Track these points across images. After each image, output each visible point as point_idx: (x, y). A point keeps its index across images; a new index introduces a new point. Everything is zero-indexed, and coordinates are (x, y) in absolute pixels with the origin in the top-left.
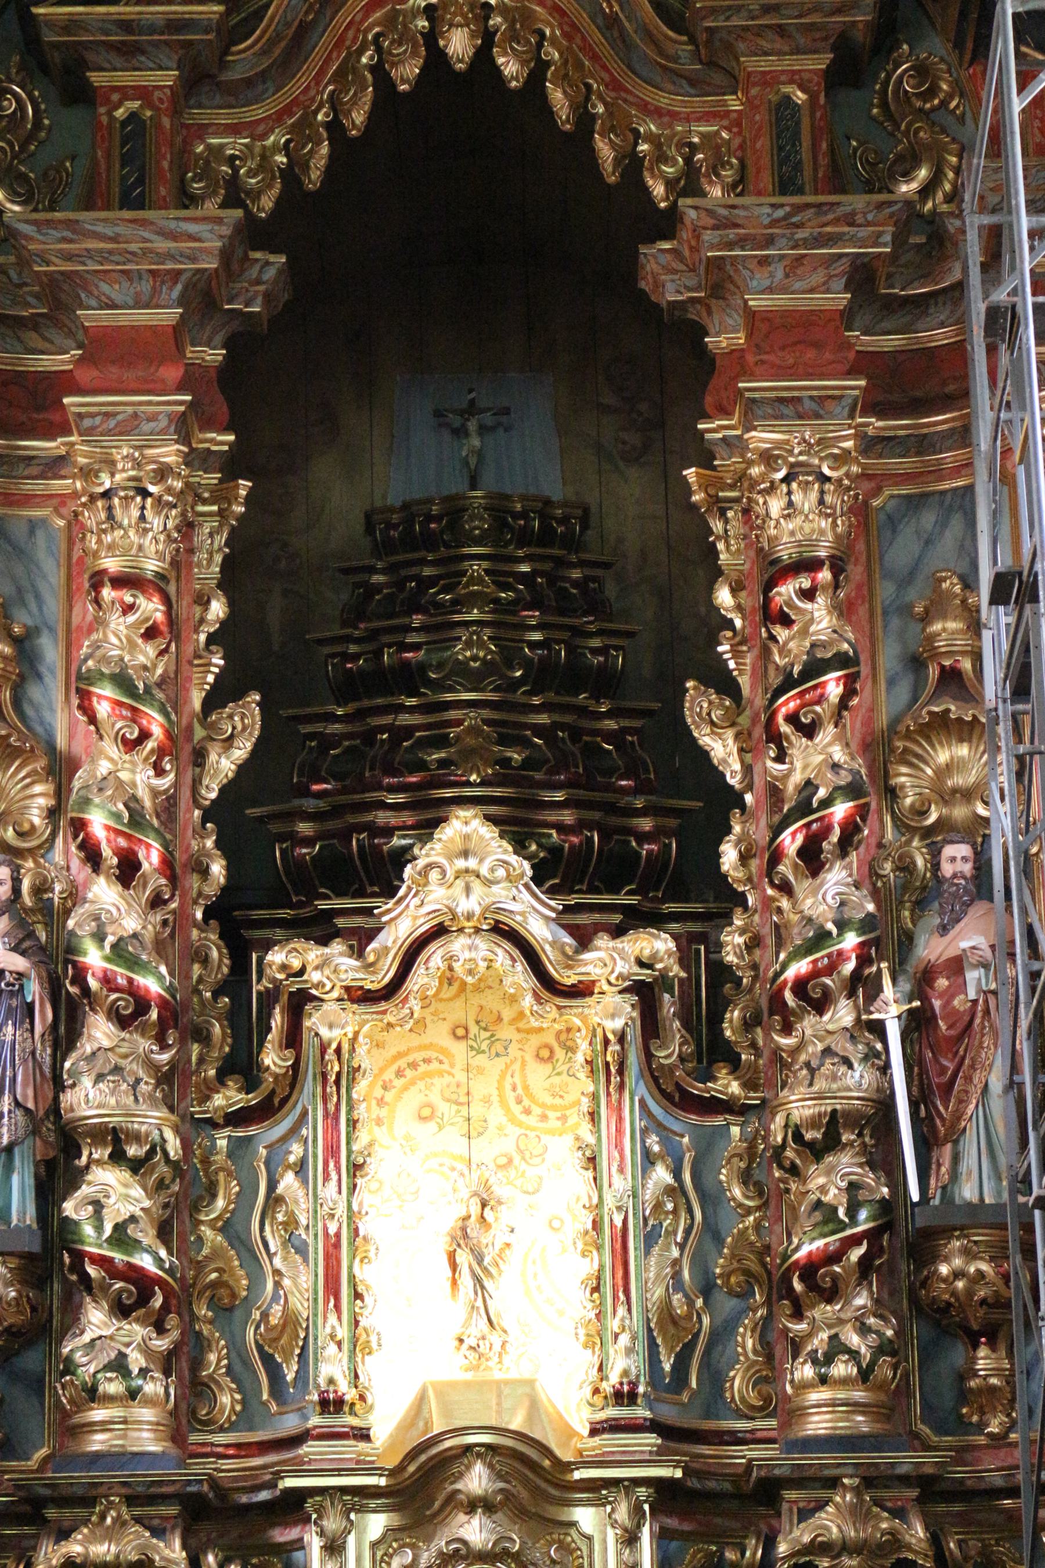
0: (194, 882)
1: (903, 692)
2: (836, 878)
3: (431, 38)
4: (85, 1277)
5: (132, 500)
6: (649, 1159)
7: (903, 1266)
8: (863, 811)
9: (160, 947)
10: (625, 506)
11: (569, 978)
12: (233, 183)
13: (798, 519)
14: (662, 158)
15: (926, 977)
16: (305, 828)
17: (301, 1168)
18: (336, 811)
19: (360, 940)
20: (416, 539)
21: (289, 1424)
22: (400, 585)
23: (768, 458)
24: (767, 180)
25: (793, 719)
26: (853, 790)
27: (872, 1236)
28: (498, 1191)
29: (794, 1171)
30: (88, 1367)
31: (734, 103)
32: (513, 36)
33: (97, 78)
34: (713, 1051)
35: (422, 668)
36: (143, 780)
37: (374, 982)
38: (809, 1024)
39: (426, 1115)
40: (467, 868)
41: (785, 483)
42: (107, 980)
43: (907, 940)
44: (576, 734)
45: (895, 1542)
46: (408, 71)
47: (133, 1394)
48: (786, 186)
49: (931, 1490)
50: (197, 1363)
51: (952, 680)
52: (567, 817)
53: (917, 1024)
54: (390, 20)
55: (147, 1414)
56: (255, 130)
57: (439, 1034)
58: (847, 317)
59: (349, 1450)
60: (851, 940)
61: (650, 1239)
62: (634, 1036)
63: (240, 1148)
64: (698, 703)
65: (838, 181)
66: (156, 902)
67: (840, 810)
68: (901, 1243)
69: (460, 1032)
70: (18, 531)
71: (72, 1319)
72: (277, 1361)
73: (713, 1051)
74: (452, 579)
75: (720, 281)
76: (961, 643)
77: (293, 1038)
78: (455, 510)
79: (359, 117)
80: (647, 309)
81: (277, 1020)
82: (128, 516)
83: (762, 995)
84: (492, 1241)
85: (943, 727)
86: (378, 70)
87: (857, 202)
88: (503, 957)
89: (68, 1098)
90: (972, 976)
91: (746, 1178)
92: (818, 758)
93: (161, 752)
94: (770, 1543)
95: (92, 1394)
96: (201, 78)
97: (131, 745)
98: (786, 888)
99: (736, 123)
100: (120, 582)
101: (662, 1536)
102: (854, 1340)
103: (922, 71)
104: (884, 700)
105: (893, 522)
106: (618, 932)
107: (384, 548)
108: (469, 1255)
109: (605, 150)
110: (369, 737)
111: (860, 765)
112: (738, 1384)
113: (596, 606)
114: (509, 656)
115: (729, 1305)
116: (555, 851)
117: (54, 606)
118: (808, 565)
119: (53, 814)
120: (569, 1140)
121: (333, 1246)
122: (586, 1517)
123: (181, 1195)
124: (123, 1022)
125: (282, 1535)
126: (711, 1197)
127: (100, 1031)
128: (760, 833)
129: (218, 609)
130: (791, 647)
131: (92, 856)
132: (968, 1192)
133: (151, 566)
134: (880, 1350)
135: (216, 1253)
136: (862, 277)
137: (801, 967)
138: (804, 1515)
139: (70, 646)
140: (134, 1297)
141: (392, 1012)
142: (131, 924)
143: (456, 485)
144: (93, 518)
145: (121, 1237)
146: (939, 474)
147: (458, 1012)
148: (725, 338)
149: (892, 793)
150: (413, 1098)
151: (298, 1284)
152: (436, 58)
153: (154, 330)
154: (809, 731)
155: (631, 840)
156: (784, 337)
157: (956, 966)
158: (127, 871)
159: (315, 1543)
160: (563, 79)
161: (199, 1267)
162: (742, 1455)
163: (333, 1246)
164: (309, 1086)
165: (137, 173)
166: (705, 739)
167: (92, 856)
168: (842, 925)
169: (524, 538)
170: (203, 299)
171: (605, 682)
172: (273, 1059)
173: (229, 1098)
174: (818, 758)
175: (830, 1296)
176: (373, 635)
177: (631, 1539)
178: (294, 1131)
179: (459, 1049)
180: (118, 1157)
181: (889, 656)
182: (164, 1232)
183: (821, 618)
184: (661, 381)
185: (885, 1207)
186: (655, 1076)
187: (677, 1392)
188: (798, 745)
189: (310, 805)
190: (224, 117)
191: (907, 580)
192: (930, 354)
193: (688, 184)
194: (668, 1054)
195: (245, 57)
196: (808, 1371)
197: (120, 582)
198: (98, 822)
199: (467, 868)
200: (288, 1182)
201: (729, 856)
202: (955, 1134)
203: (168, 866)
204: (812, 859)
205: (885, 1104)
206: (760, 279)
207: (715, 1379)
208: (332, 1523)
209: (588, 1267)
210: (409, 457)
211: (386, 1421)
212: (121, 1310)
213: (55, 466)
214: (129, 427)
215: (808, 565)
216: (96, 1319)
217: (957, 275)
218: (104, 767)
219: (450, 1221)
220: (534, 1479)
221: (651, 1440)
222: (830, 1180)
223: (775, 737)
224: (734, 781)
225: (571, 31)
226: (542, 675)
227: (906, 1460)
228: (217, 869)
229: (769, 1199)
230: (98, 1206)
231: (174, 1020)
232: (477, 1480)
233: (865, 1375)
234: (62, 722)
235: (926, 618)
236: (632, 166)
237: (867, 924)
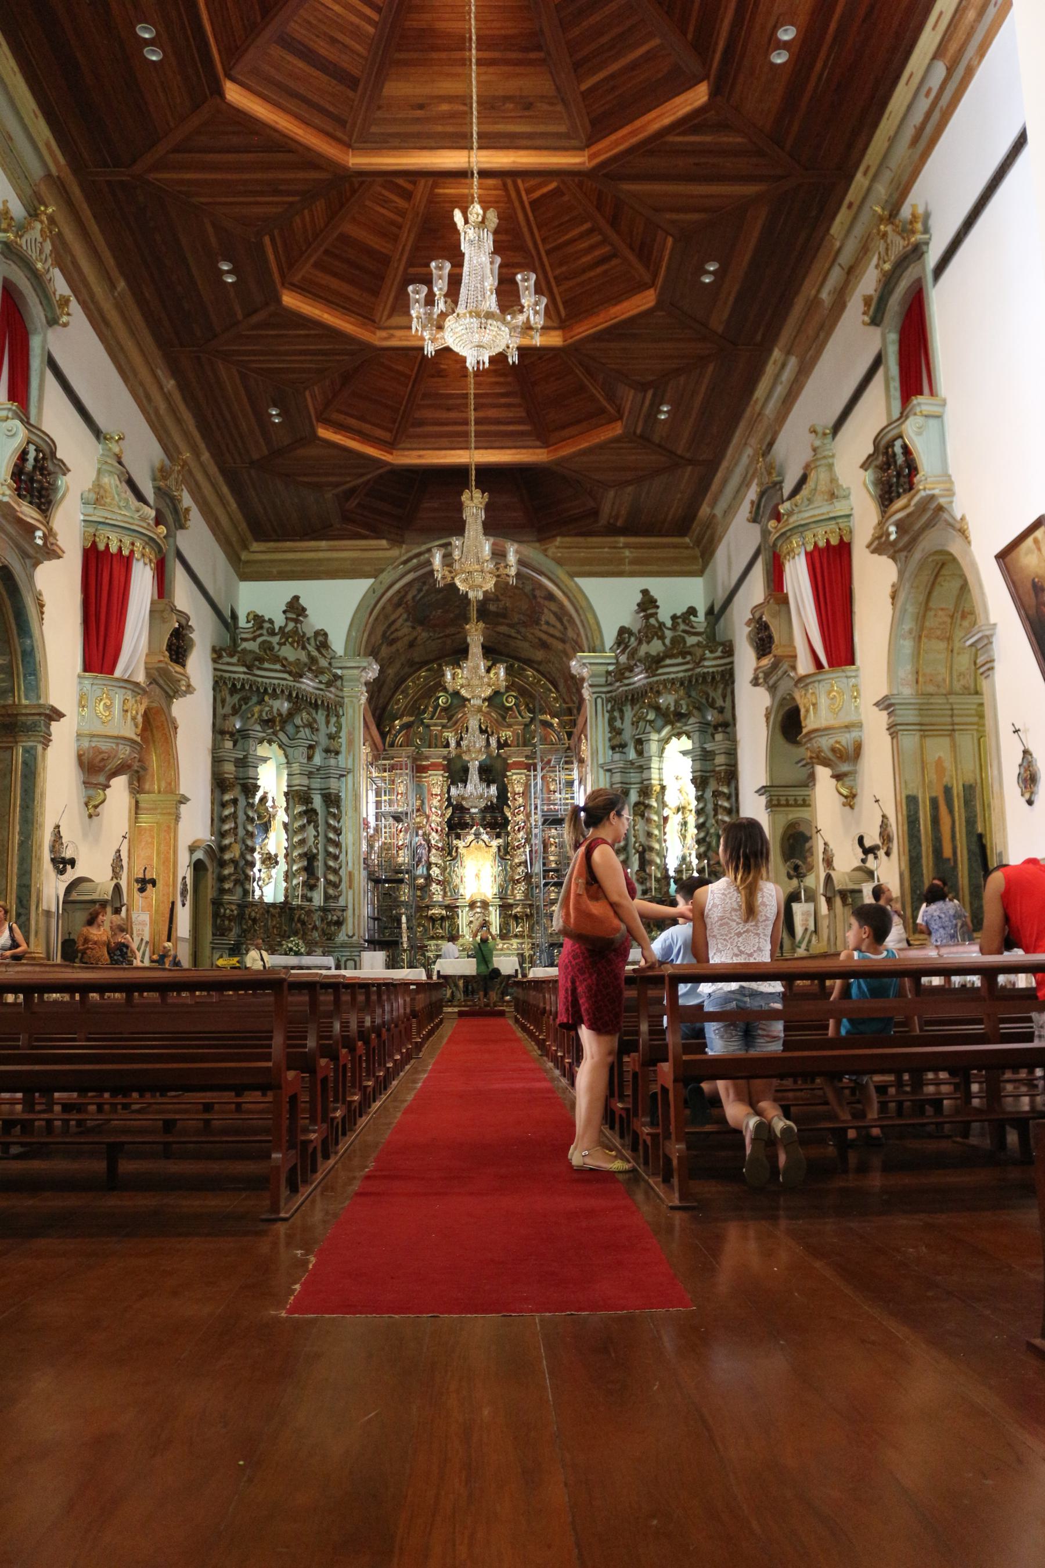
2: (522, 833)
13: (519, 789)
34: (507, 853)
49: (531, 906)
53: (531, 851)
68: (528, 877)
72: (455, 890)
73: (507, 853)
123: (443, 870)
127: (434, 851)
139: (429, 800)
140: (439, 883)
151: (457, 881)
158: (437, 831)
172: (454, 854)
173: (449, 858)
187: (502, 895)
198: (433, 825)
211: (468, 898)
216: (434, 885)
220: (485, 905)
222: (521, 869)
232: (479, 904)
234: (427, 811)
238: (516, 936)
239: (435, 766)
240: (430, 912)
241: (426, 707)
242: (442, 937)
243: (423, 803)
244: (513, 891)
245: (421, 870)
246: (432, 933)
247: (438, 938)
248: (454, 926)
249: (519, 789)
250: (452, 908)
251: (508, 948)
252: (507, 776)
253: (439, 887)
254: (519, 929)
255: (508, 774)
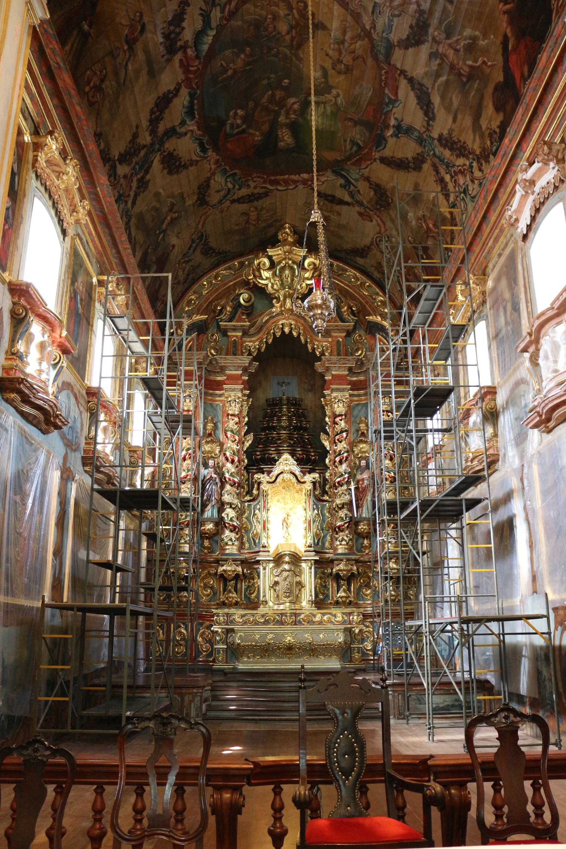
0: (242, 463)
1: (355, 435)
3: (282, 329)
4: (226, 527)
5: (234, 401)
6: (314, 509)
7: (354, 527)
8: (349, 455)
9: (237, 473)
10: (309, 399)
11: (302, 481)
12: (250, 350)
13: (340, 408)
14: (318, 348)
15: (358, 482)
16: (258, 453)
17: (259, 509)
18: (263, 451)
19: (269, 473)
20: (274, 404)
21: (257, 549)
22: (272, 412)
23: (335, 398)
24: (335, 353)
25: (338, 440)
26: (347, 452)
27: (349, 522)
28: (290, 514)
29: (337, 512)
30: (226, 540)
31: (330, 340)
32: (295, 329)
33: (229, 334)
34: (324, 492)
35: (276, 426)
36: (235, 447)
37: (271, 481)
38: (339, 489)
39: (278, 501)
40: (286, 463)
41: (337, 401)
42: (229, 479)
43: (355, 475)
44: (301, 438)
45: (351, 569)
46: (278, 334)
47: (233, 544)
48: (339, 355)
49: (357, 561)
50: (242, 540)
51: (363, 434)
52: (300, 453)
53: (357, 489)
54: (275, 326)
55: (235, 547)
56: (254, 342)
57: (281, 488)
58: (348, 375)
59: (266, 554)
60: (347, 475)
61: (314, 522)
62: (312, 490)
63: (249, 506)
64: (323, 436)
65: (346, 355)
66: (237, 467)
67: (345, 455)
68: (353, 523)
69: (284, 488)
70: (215, 406)
71: (223, 533)
72: (255, 540)
73: (324, 492)
74: (281, 411)
75: (328, 369)
76: (365, 428)
77: (258, 489)
78: (281, 399)
79: (271, 341)
80: (314, 371)
81: (256, 486)
82: (233, 405)
83: (332, 483)
84: (289, 522)
85: (361, 442)
86: (274, 333)
87: (350, 358)
88: (291, 477)
89: (223, 498)
90: (366, 482)
91: (329, 512)
92: (342, 446)
93: (238, 443)
94: (332, 569)
95: (227, 544)
96: (246, 333)
97: (233, 442)
98: (336, 467)
99: (330, 343)
100: (232, 415)
101: (315, 568)
102: (346, 538)
103: (360, 336)
104: (352, 437)
105: (354, 408)
106: (310, 473)
107: (269, 405)
108: (285, 522)
109: (309, 346)
110: (268, 438)
111: (348, 447)
112: (327, 544)
113: (304, 416)
114: (290, 425)
115: (325, 532)
116: (298, 458)
117: (220, 418)
118: (341, 415)
119: (220, 452)
120: (301, 506)
121: (264, 522)
122: (304, 565)
123: (240, 513)
124: (232, 486)
125: (256, 566)
126: (323, 515)
127: (228, 487)
128: (332, 457)
129: (246, 419)
130: (338, 428)
131: (227, 459)
132: (364, 515)
133: (237, 413)
134: (350, 540)
135: (245, 522)
136: (350, 369)
137: (339, 479)
138: (337, 565)
139: (223, 424)
140: (233, 529)
141: (274, 485)
142: (233, 470)
143: (281, 395)
144: (227, 405)
145: (231, 520)
146: (361, 400)
147: (284, 485)
148: (328, 378)
149: (353, 452)
150: (276, 498)
151: (259, 528)
152: (283, 332)
153: (237, 375)
154: (341, 442)
155: (312, 458)
156: (338, 379)
157: (363, 480)
158: (233, 462)
159: (261, 568)
160: (303, 335)
161: (243, 524)
162: (327, 556)
163: (264, 522)
164: (261, 497)
165: (235, 349)
166: (324, 442)
167: (227, 459)
168: (345, 473)
169: (292, 404)
170: (245, 370)
171: (305, 429)
172: (255, 492)
173: (248, 498)
174: (342, 446)
175: (342, 531)
176: (268, 421)
177: (311, 568)
178: (258, 503)
179: (284, 491)
180: (231, 507)
181: (353, 430)
182: (237, 519)
183: (343, 424)
184: (318, 384)
185: (351, 518)
186: (315, 496)
187: (318, 546)
188: (339, 444)
189: (259, 449)
190: (249, 339)
191: (356, 417)
192: (360, 381)
193: (323, 354)
194: (317, 493)
195: (252, 331)
196: (338, 543)
197: (232, 415)
198: (228, 454)
199: (286, 463)
200: (257, 511)
201: (327, 461)
202: (362, 506)
203: (239, 461)
204: (341, 462)
205: (351, 501)
206: (334, 369)
207: (323, 544)
208: (264, 565)
209: (305, 526)
210: (272, 390)
211: (272, 549)
212: (231, 531)
213: (220, 396)
214: (234, 390)
215: (341, 415)
216: (227, 532)
217: (365, 369)
218: (229, 445)
219: (282, 518)
220: (296, 559)
221: (314, 553)
222: (342, 513)
223: (335, 442)
224: (328, 449)
225: (305, 328)
226: (296, 428)
227: (353, 557)
228: (246, 461)
229: (332, 515)
230: (228, 515)
231: (239, 485)
232: (287, 559)
233: (347, 544)
234: (222, 437)
235: (359, 424)
236: (314, 349)
237: (349, 473)
238: (337, 603)
239: (233, 379)
240: (221, 569)
241: (223, 308)
242: (237, 603)
243: (216, 427)
244: (332, 543)
245: (210, 512)
246: (222, 598)
247: (230, 606)
248: (252, 588)
249: (340, 408)
250: (251, 565)
251: (330, 621)
252: (324, 396)
253: (233, 535)
254: (342, 594)
255: (326, 392)
